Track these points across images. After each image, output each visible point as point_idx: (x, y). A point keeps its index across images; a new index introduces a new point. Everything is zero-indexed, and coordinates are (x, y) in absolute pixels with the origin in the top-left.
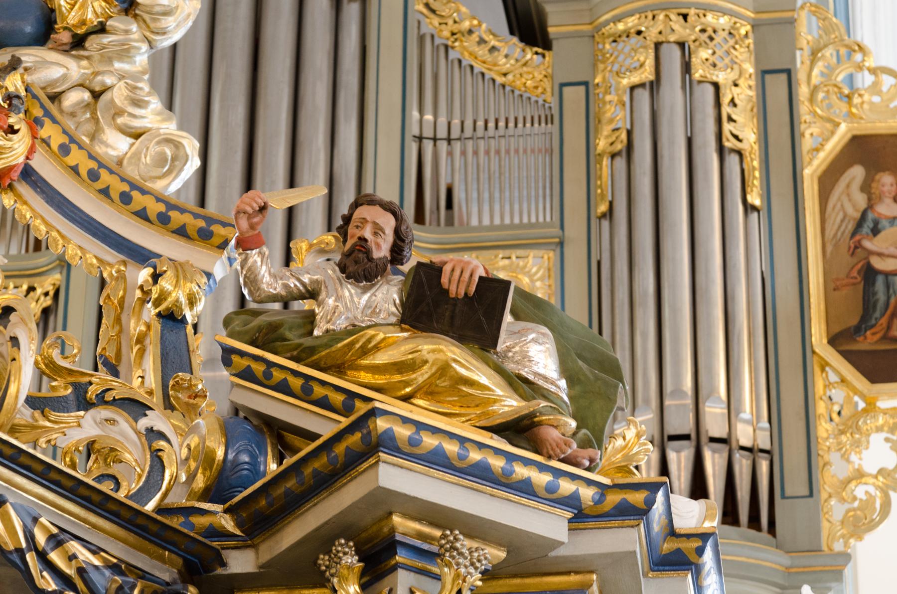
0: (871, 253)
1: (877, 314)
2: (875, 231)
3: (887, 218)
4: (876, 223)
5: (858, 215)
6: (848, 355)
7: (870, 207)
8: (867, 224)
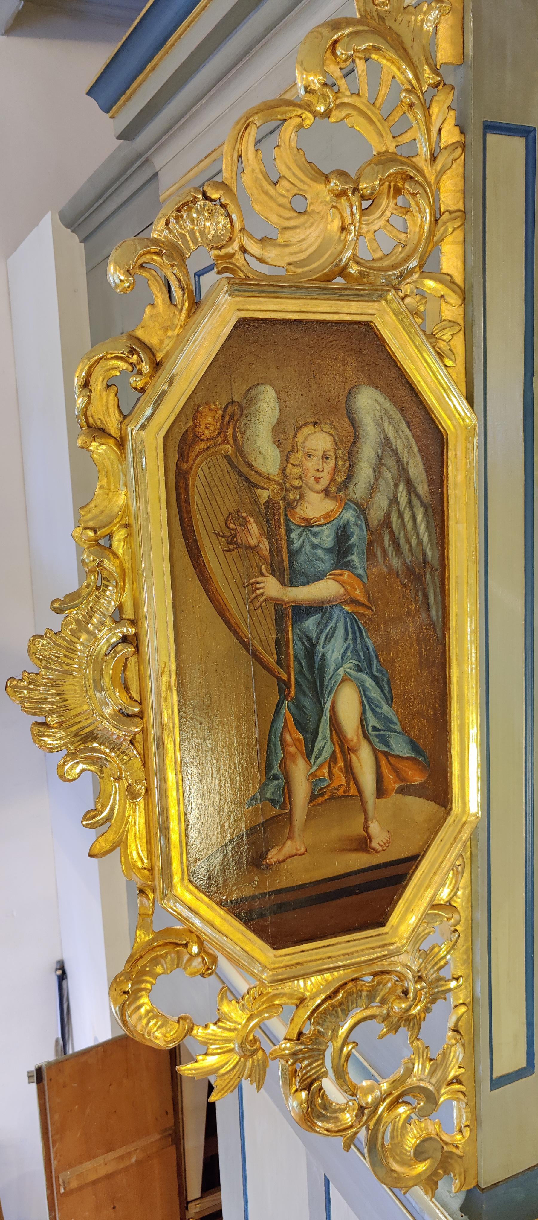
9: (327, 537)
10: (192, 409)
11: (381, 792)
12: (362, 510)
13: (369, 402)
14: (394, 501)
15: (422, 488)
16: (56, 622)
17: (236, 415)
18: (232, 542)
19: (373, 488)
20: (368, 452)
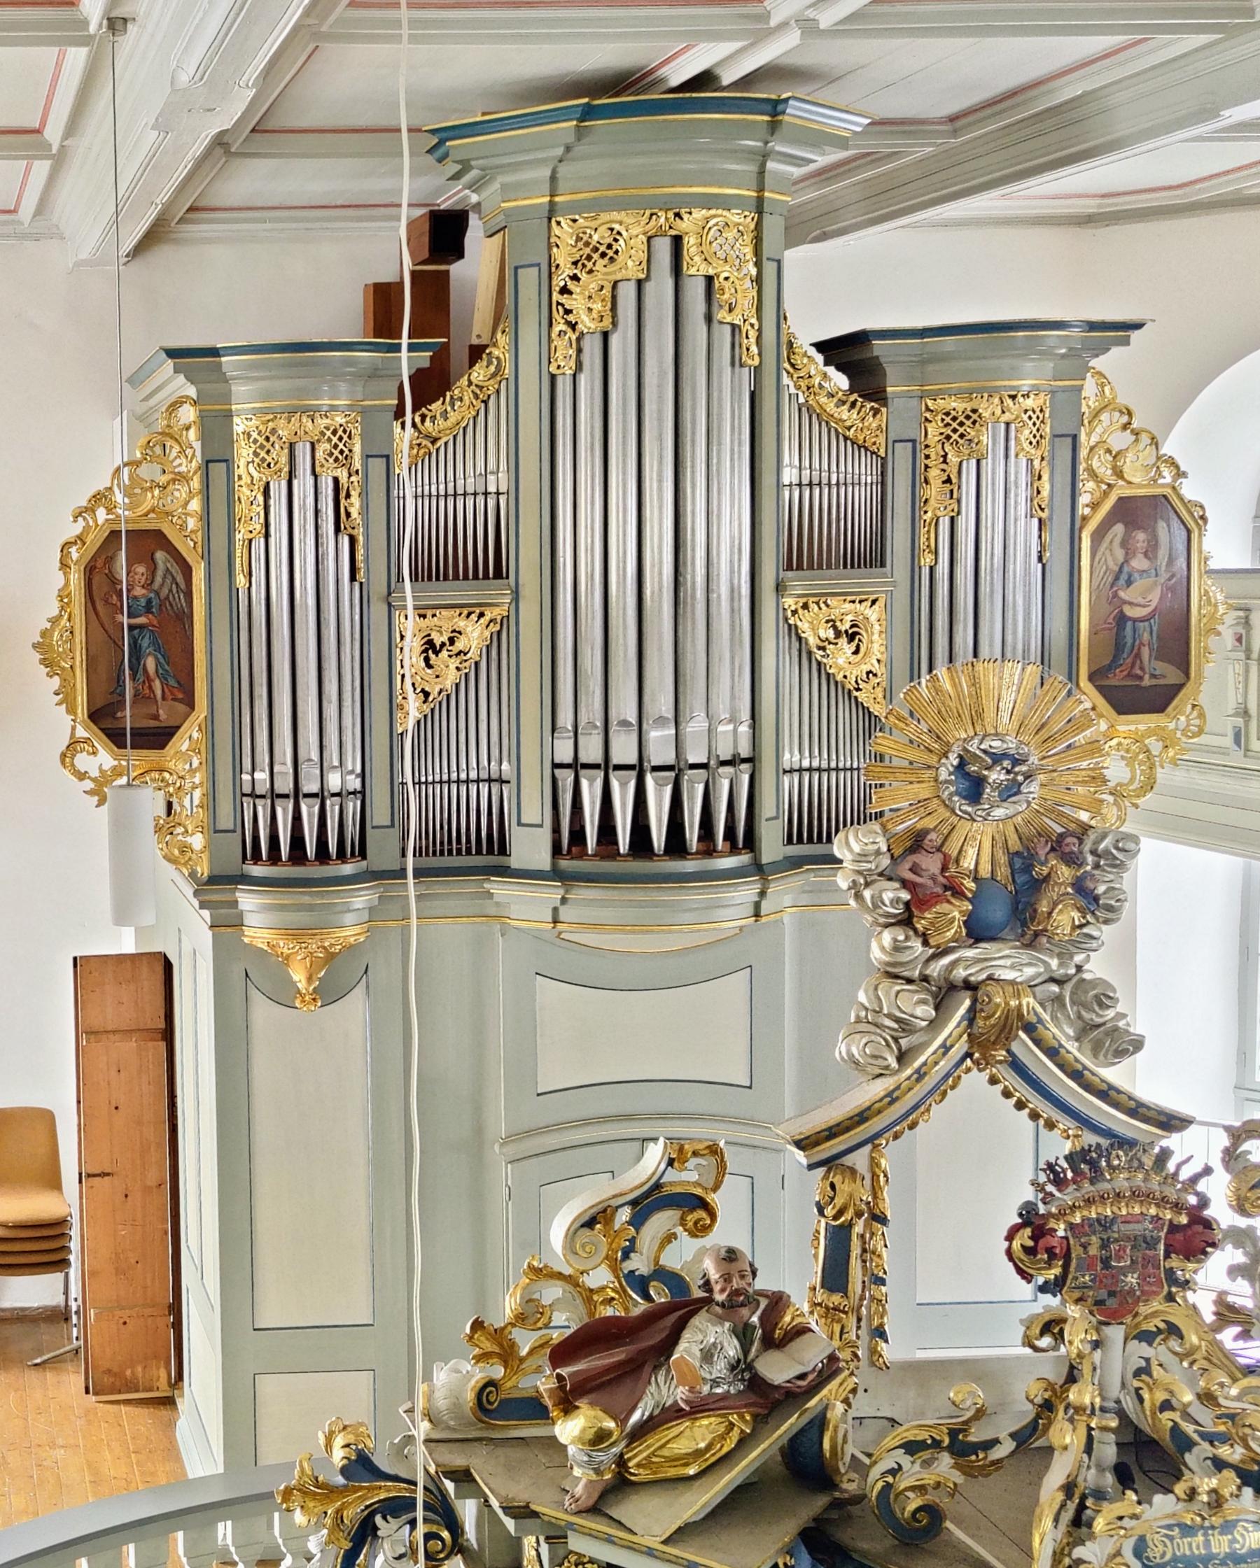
0: (1125, 602)
1: (1125, 655)
2: (1129, 583)
3: (1138, 571)
4: (1130, 576)
5: (1117, 569)
6: (1101, 689)
7: (1126, 561)
8: (1121, 576)
9: (143, 602)
10: (94, 558)
11: (164, 698)
12: (157, 593)
13: (160, 556)
14: (171, 590)
15: (183, 586)
16: (48, 625)
17: (111, 560)
18: (107, 602)
19: (162, 585)
20: (160, 573)
